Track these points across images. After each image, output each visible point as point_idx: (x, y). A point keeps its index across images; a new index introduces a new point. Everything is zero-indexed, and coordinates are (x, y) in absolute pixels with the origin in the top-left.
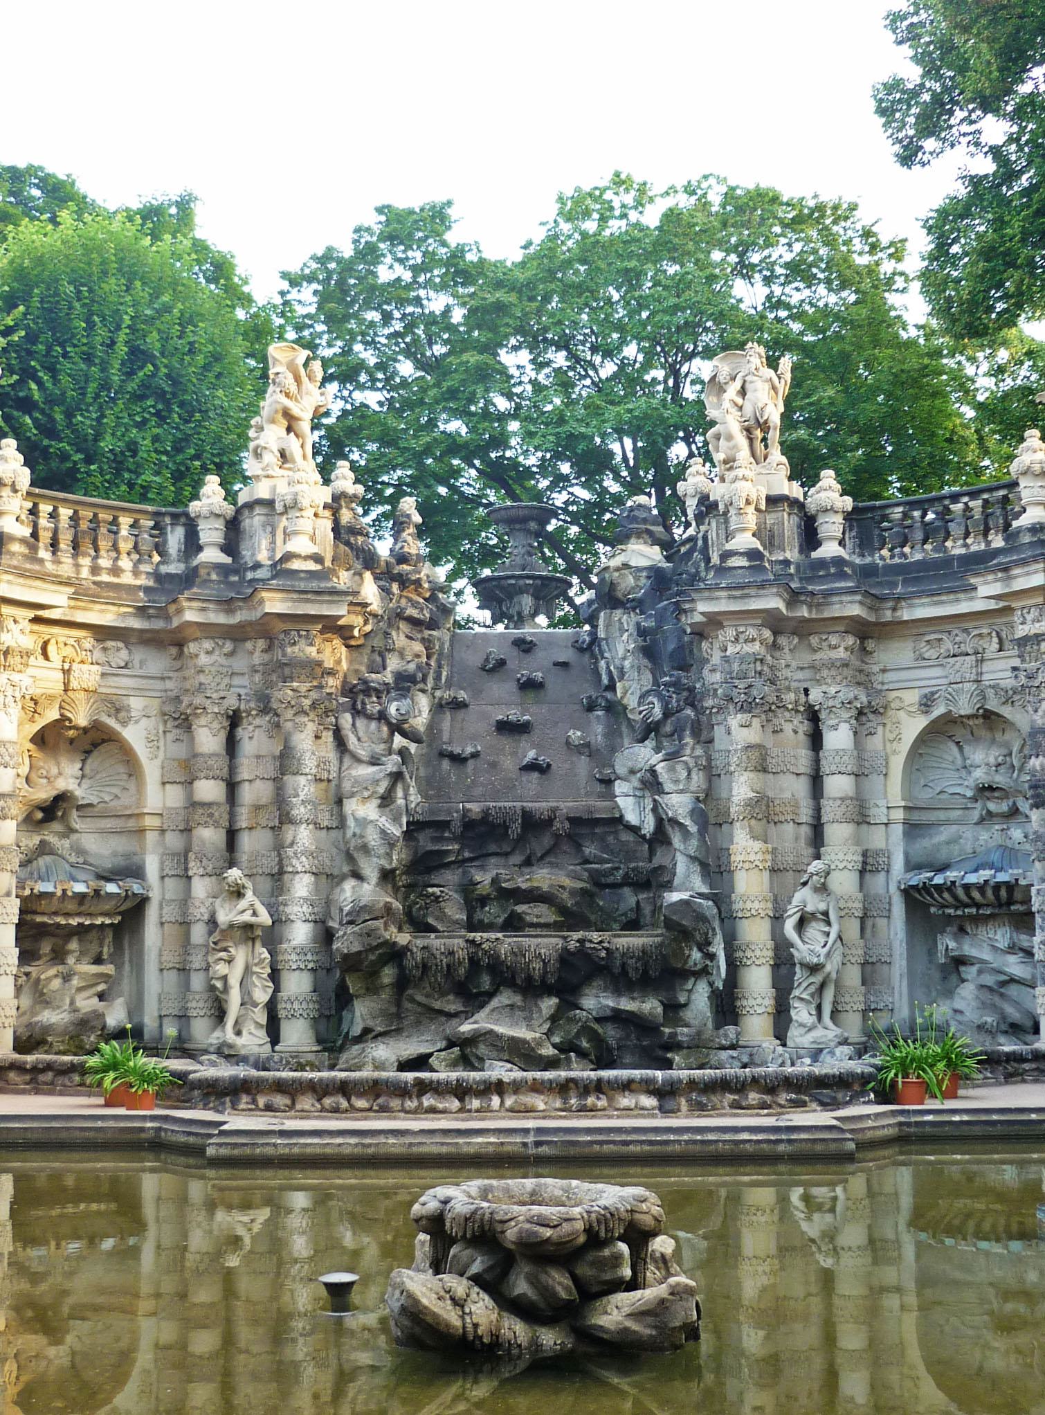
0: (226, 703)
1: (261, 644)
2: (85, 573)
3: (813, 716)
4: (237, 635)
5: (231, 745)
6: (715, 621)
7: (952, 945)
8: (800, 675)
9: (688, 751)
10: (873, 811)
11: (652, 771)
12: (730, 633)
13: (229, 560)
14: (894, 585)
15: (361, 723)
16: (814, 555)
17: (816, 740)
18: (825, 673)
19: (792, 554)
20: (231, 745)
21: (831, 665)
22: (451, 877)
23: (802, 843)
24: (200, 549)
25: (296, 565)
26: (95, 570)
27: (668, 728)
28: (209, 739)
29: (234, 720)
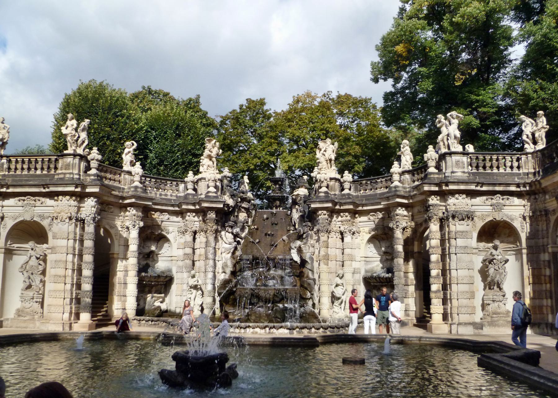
0: (193, 229)
1: (202, 214)
2: (158, 196)
3: (342, 233)
4: (196, 212)
5: (194, 239)
6: (317, 209)
7: (376, 292)
8: (338, 223)
9: (309, 242)
10: (357, 258)
11: (300, 247)
12: (320, 212)
13: (194, 193)
14: (362, 200)
15: (227, 234)
16: (342, 193)
17: (342, 239)
18: (344, 223)
19: (337, 192)
20: (194, 239)
21: (346, 221)
22: (248, 273)
23: (338, 266)
24: (187, 190)
25: (210, 194)
26: (161, 195)
27: (304, 236)
28: (189, 237)
29: (195, 233)
